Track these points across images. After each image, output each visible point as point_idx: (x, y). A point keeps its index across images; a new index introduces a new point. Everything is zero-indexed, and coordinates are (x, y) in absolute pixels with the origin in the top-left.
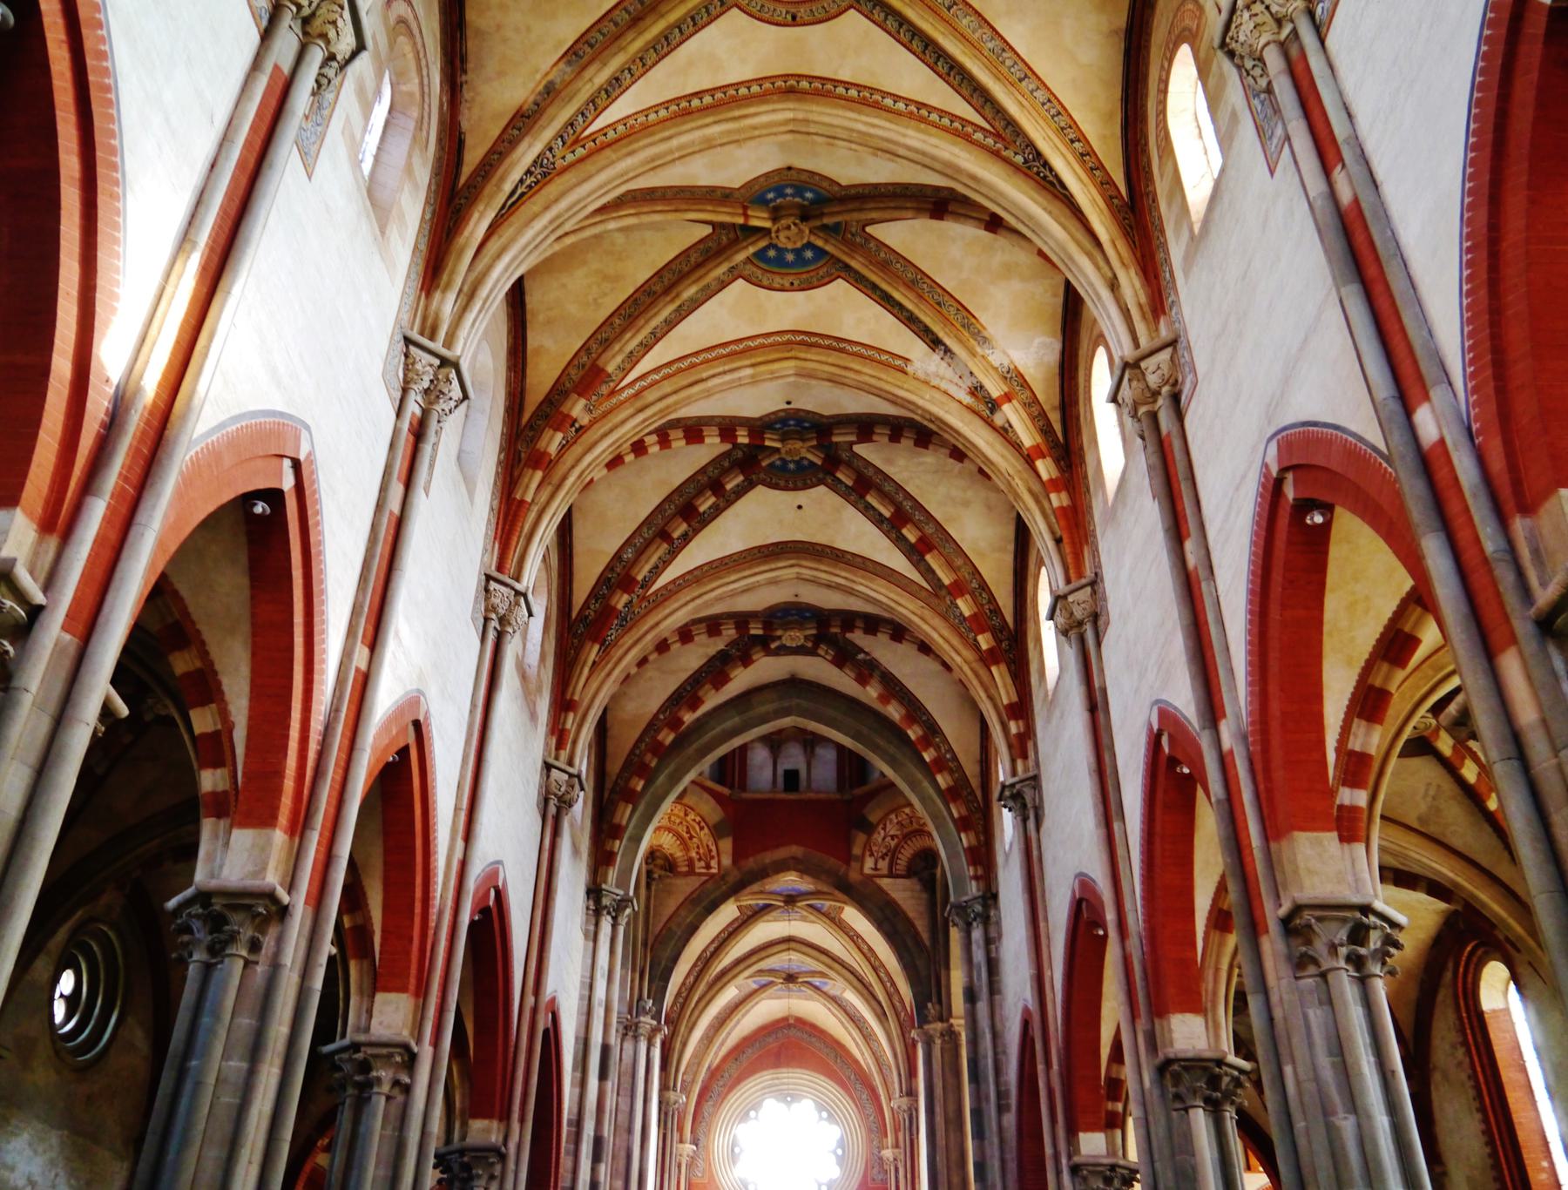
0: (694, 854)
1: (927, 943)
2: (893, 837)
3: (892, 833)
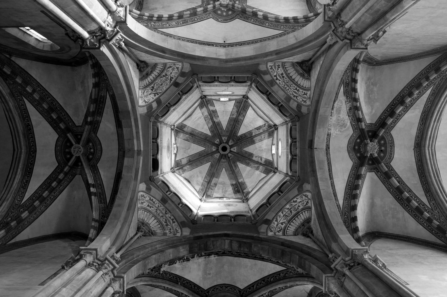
0: (167, 232)
1: (317, 249)
2: (282, 224)
3: (281, 222)
